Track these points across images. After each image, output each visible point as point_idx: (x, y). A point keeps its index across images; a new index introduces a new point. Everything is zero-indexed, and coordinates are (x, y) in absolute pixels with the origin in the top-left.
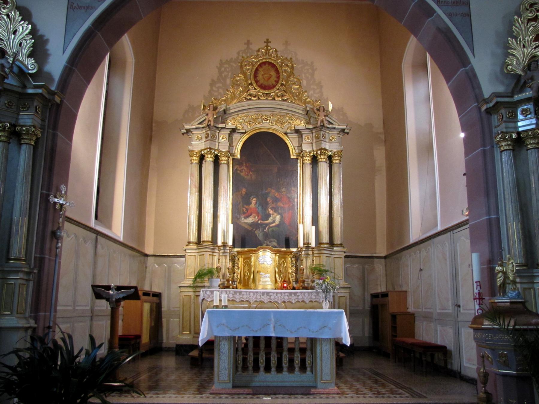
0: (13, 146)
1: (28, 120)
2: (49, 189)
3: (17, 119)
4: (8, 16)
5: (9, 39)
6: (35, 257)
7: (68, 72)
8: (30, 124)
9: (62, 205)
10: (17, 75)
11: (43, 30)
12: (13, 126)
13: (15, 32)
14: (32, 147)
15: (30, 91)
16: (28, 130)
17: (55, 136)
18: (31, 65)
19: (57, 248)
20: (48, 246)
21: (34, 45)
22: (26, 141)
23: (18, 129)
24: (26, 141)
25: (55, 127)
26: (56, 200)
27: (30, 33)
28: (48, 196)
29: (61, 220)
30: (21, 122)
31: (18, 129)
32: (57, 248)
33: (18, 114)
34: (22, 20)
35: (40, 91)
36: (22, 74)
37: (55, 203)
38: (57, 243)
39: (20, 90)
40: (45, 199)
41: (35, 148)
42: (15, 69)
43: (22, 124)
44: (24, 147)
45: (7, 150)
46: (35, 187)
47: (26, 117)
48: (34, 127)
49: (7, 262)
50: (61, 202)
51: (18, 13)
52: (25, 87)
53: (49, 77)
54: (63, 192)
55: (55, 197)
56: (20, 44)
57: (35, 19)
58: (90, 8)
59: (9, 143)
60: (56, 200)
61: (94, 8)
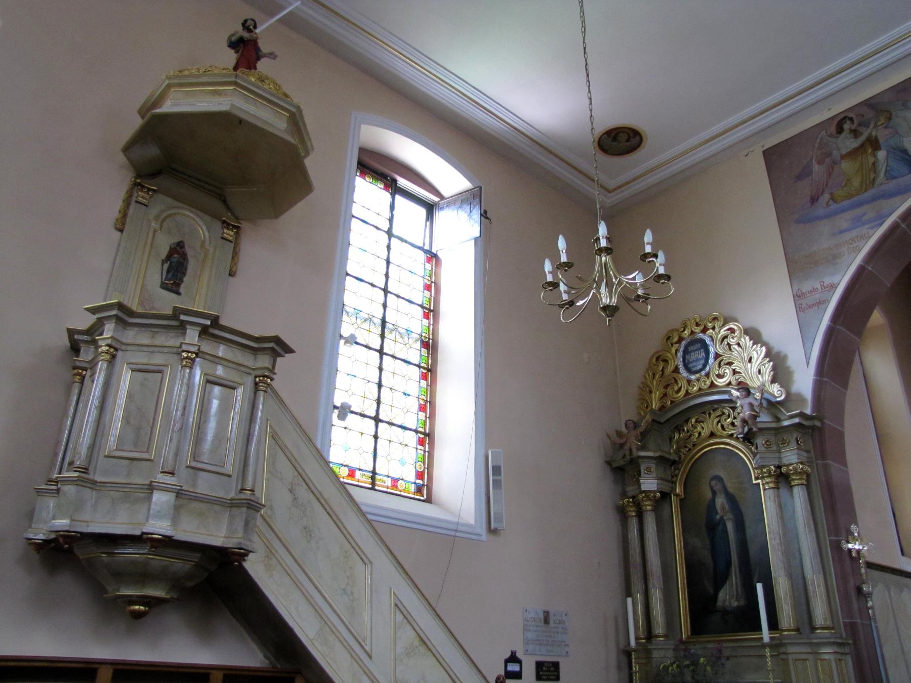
0: (784, 491)
1: (791, 457)
2: (837, 534)
3: (780, 458)
4: (739, 344)
5: (747, 370)
6: (844, 623)
7: (819, 386)
8: (796, 461)
9: (858, 551)
10: (767, 409)
11: (777, 346)
12: (779, 467)
13: (750, 360)
14: (804, 487)
15: (786, 423)
16: (795, 469)
17: (826, 467)
18: (776, 391)
19: (868, 609)
20: (855, 606)
21: (774, 368)
22: (796, 482)
23: (784, 470)
24: (796, 482)
25: (823, 455)
26: (850, 546)
27: (766, 356)
28: (838, 543)
29: (863, 571)
30: (785, 461)
31: (784, 470)
32: (868, 609)
33: (780, 452)
34: (754, 344)
35: (797, 420)
36: (773, 406)
37: (850, 550)
38: (867, 602)
39: (774, 425)
40: (837, 547)
41: (808, 487)
42: (765, 403)
43: (787, 463)
44: (796, 490)
45: (779, 496)
46: (821, 536)
47: (788, 454)
48: (802, 463)
49: (812, 633)
50: (857, 547)
51: (747, 338)
52: (778, 420)
53: (800, 399)
54: (856, 534)
55: (848, 542)
56: (759, 372)
57: (766, 336)
58: (822, 303)
59: (778, 488)
60: (850, 546)
61: (826, 302)
